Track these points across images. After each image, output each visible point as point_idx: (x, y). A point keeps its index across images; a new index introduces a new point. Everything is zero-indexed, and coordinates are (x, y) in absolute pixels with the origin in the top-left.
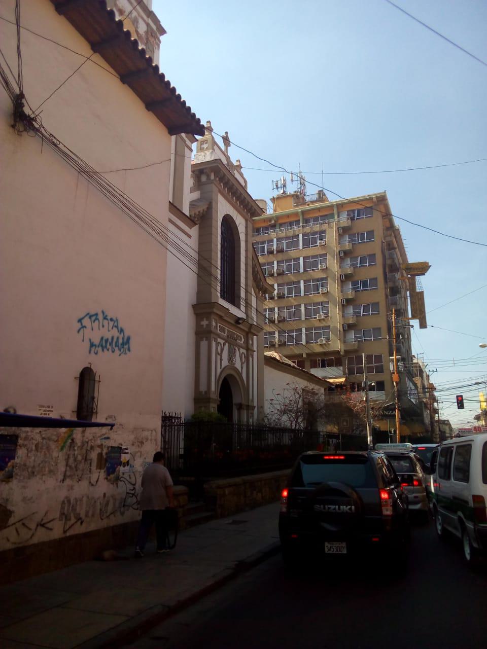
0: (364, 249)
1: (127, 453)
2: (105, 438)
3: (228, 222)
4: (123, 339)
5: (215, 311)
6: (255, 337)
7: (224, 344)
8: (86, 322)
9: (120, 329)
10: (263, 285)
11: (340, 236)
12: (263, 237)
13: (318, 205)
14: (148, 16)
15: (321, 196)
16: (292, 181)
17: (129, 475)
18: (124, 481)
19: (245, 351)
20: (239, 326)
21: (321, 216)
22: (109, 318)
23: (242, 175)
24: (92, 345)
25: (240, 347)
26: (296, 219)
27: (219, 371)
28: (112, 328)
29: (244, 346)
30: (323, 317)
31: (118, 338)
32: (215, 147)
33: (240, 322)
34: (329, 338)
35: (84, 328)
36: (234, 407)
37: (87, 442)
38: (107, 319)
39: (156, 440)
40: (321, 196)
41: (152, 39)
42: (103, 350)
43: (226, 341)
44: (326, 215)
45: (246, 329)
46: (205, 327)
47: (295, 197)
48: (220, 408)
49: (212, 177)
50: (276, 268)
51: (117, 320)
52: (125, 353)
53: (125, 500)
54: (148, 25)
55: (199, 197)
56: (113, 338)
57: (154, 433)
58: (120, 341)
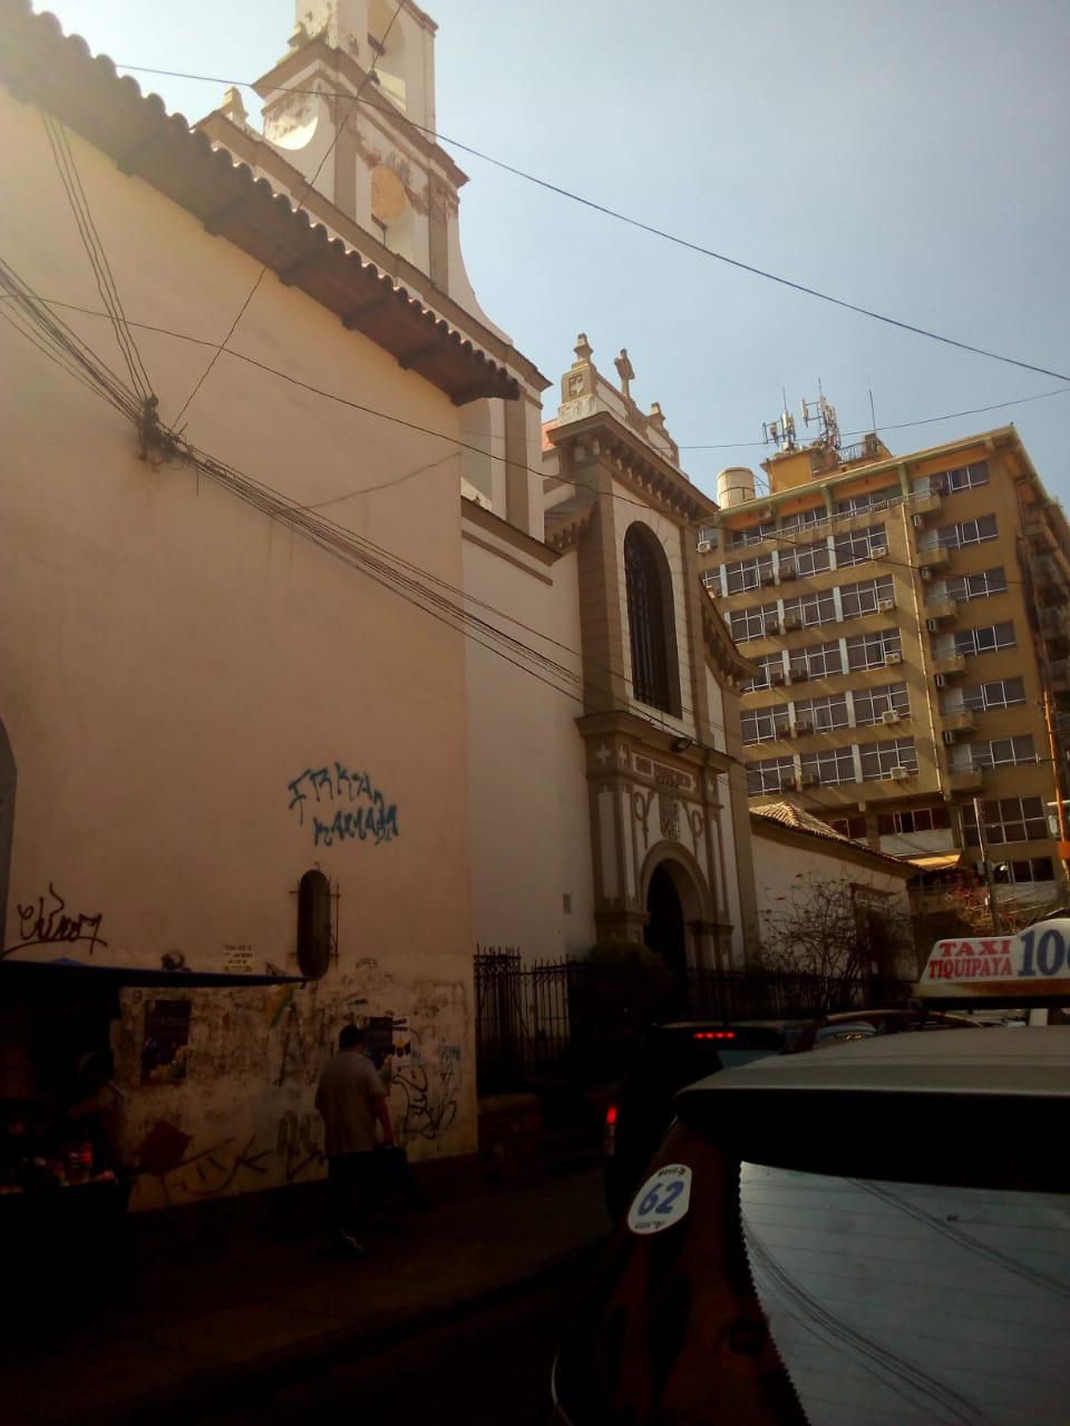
0: (980, 558)
1: (405, 1029)
2: (357, 1002)
3: (639, 537)
4: (381, 811)
5: (621, 728)
6: (724, 776)
7: (651, 796)
8: (306, 787)
9: (373, 792)
10: (732, 662)
11: (919, 534)
12: (749, 548)
13: (868, 467)
14: (428, 155)
15: (873, 446)
16: (806, 419)
18: (403, 1085)
19: (699, 809)
20: (683, 755)
21: (873, 493)
22: (349, 774)
23: (664, 434)
24: (319, 828)
25: (686, 799)
26: (814, 505)
27: (642, 853)
28: (358, 793)
29: (698, 797)
30: (895, 718)
31: (371, 811)
33: (681, 746)
34: (914, 765)
35: (303, 800)
36: (687, 929)
37: (323, 1011)
38: (347, 778)
39: (464, 1004)
40: (873, 446)
41: (439, 200)
42: (342, 837)
43: (653, 789)
44: (883, 491)
45: (698, 761)
46: (604, 762)
47: (814, 455)
48: (650, 934)
49: (597, 451)
50: (781, 617)
51: (367, 777)
52: (388, 839)
54: (430, 173)
55: (574, 494)
56: (360, 812)
58: (376, 816)
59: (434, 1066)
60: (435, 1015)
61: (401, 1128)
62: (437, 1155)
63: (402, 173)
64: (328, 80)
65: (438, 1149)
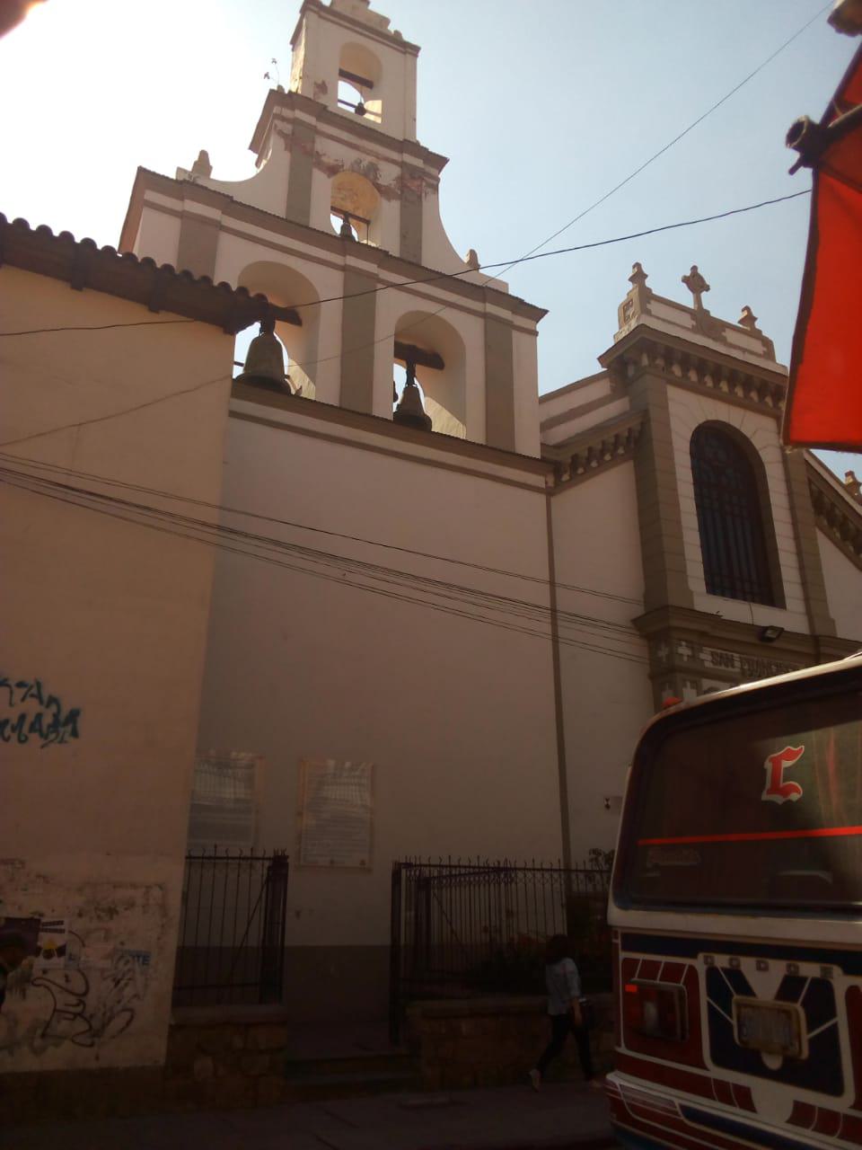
1: (62, 931)
4: (56, 716)
5: (675, 623)
9: (45, 698)
14: (401, 151)
17: (66, 977)
20: (775, 644)
22: (12, 683)
23: (757, 335)
31: (39, 716)
32: (653, 306)
33: (769, 634)
39: (163, 908)
41: (413, 185)
51: (39, 685)
52: (62, 741)
53: (48, 1024)
56: (22, 717)
57: (156, 892)
58: (47, 720)
59: (103, 970)
60: (111, 918)
61: (39, 1032)
62: (93, 1065)
63: (371, 173)
64: (283, 119)
65: (97, 1058)
